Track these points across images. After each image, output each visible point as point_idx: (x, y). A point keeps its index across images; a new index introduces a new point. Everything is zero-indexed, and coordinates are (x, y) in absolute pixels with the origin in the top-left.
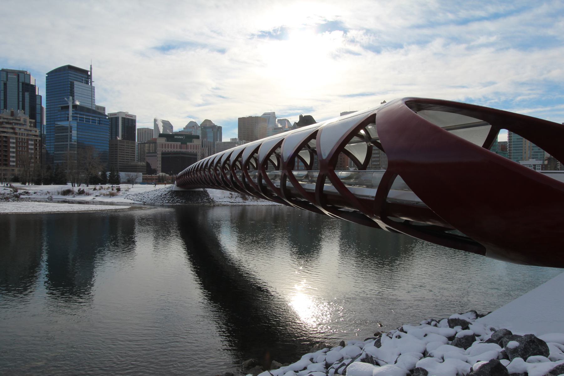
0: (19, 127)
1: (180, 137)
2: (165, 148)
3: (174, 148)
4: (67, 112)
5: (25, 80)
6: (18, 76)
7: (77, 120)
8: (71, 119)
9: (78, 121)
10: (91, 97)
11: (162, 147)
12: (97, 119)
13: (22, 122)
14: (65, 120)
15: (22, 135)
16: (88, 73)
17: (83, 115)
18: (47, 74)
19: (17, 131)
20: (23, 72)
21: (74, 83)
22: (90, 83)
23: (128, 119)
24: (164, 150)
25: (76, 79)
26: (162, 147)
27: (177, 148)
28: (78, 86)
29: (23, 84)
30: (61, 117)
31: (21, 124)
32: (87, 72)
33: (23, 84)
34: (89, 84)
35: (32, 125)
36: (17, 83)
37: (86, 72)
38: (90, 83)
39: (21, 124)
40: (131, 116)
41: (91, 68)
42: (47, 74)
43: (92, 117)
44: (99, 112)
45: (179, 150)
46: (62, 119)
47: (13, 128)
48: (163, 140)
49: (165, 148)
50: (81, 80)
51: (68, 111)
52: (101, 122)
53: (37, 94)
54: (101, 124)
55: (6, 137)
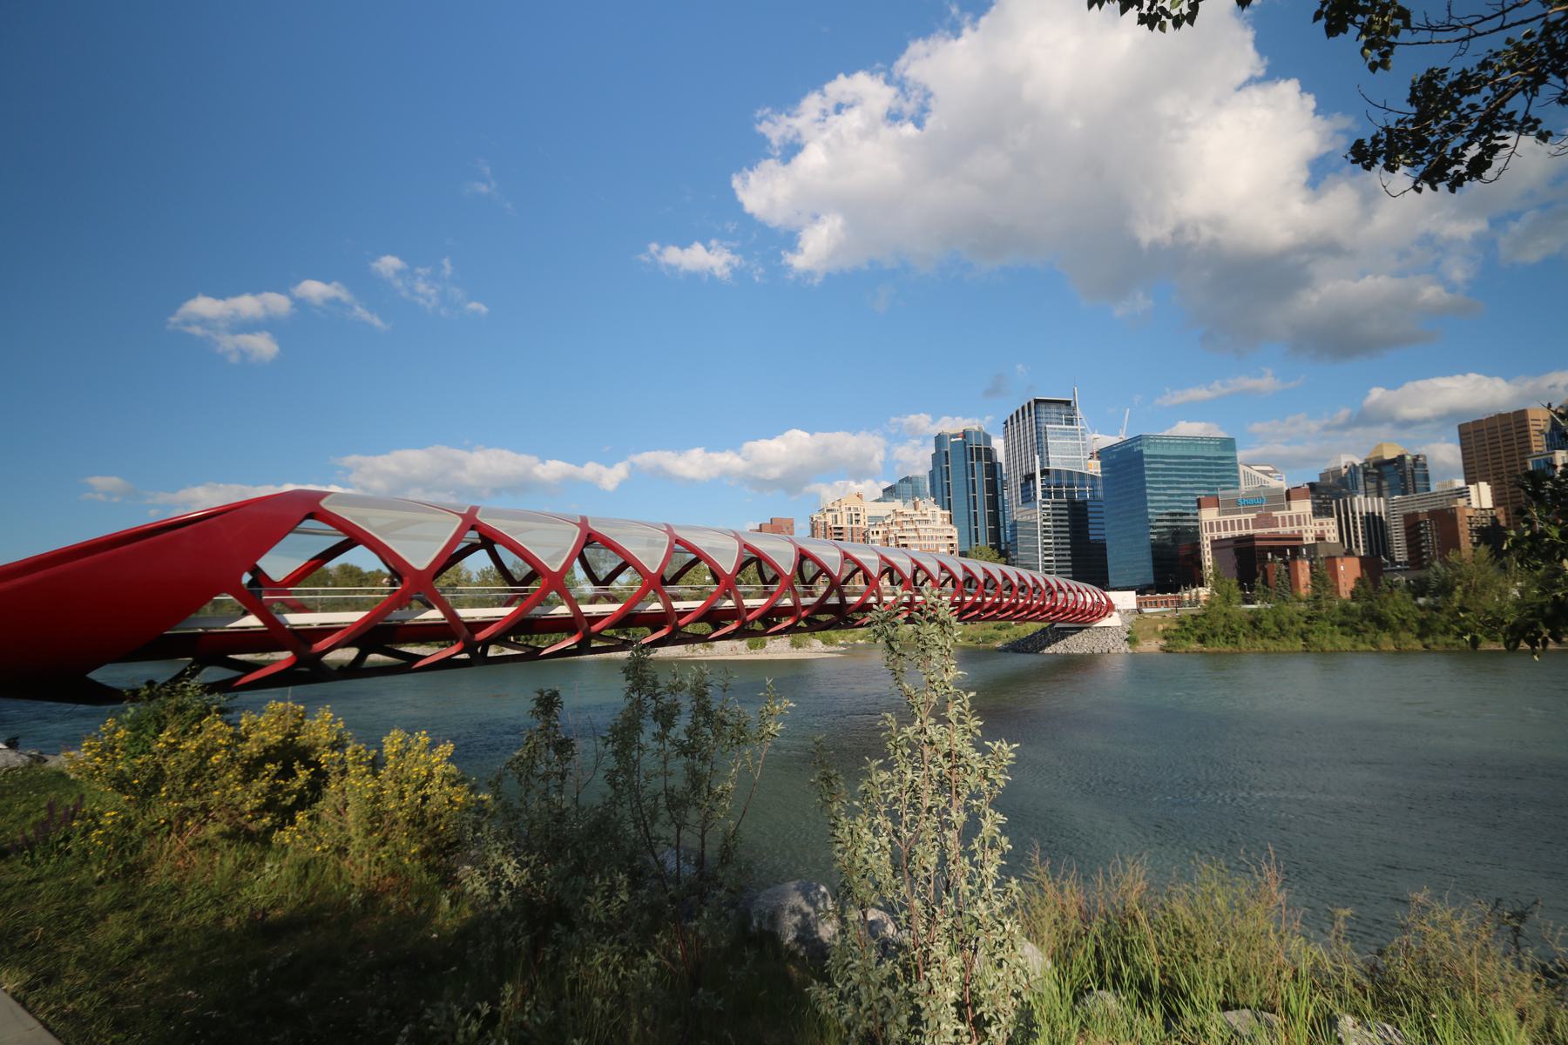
2: (1219, 530)
3: (1233, 529)
11: (1212, 530)
24: (1216, 535)
26: (1212, 530)
27: (1247, 528)
31: (927, 522)
39: (927, 522)
45: (1251, 531)
49: (1219, 530)
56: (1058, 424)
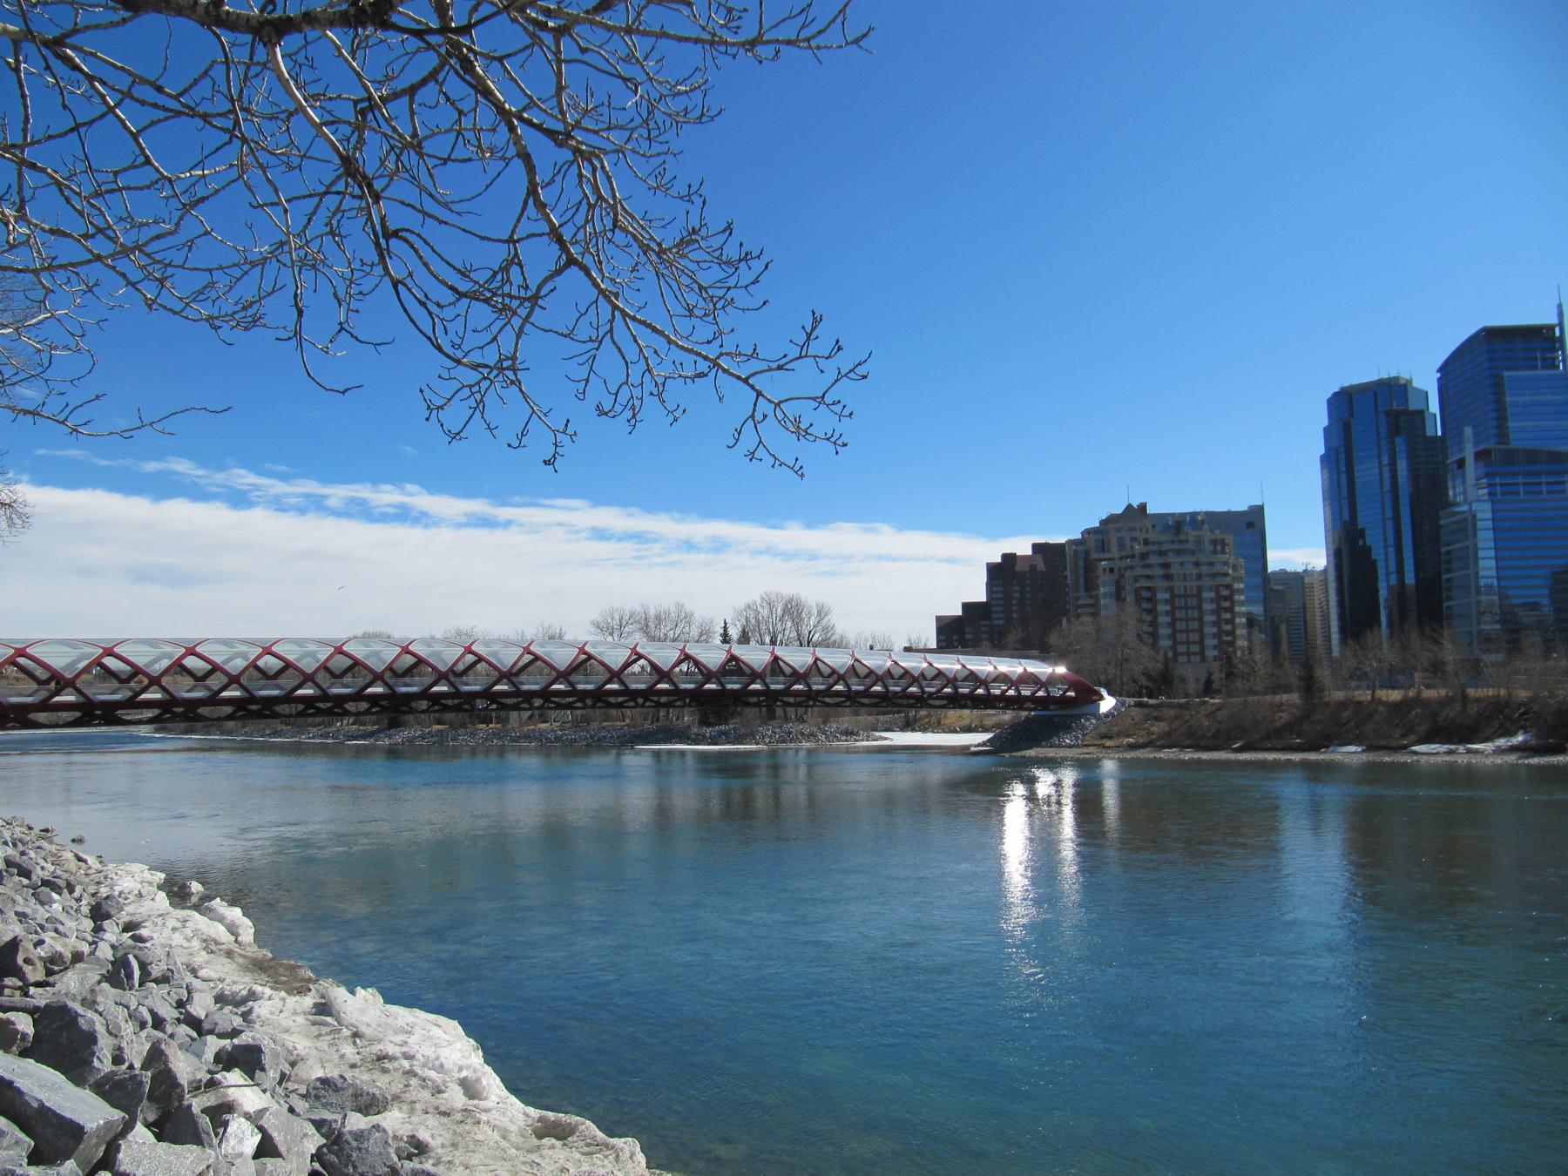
13: (1191, 546)
15: (1185, 579)
16: (1554, 333)
19: (1175, 570)
21: (1503, 377)
22: (1561, 364)
31: (1186, 551)
32: (1551, 328)
33: (1388, 414)
38: (1561, 364)
41: (1561, 315)
47: (1166, 566)
55: (1149, 589)
56: (1527, 368)
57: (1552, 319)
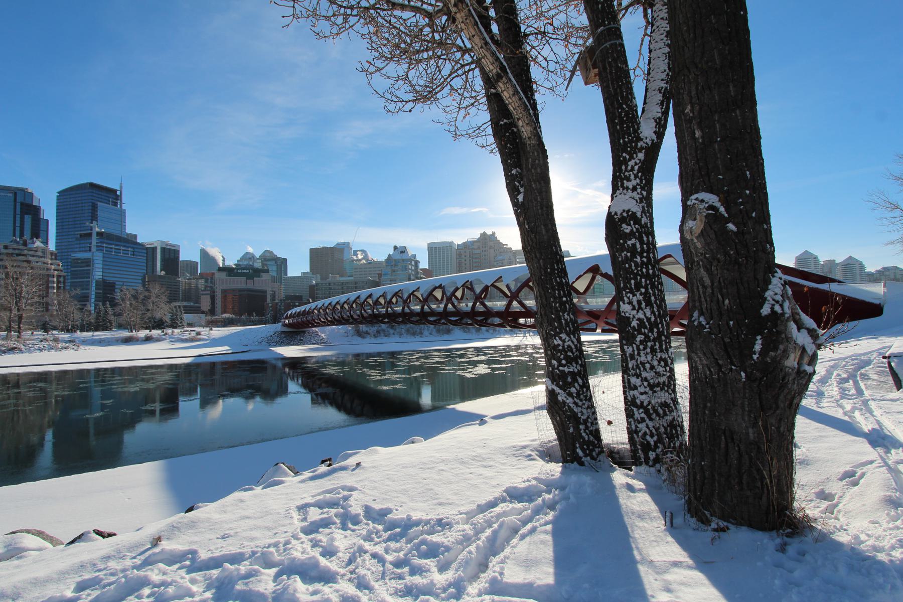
0: (34, 259)
1: (245, 271)
4: (89, 241)
5: (24, 199)
6: (15, 194)
7: (103, 250)
8: (94, 249)
9: (104, 252)
10: (120, 223)
12: (130, 249)
13: (39, 253)
14: (86, 251)
17: (112, 244)
18: (58, 193)
20: (23, 191)
23: (170, 249)
25: (100, 200)
28: (103, 209)
29: (22, 204)
30: (79, 248)
32: (115, 191)
34: (117, 206)
35: (53, 257)
36: (13, 204)
37: (114, 191)
40: (174, 246)
41: (121, 187)
42: (58, 193)
43: (124, 246)
44: (130, 241)
46: (81, 249)
48: (223, 275)
50: (107, 201)
51: (91, 239)
52: (135, 253)
53: (42, 217)
54: (136, 255)
56: (106, 203)
57: (117, 187)
